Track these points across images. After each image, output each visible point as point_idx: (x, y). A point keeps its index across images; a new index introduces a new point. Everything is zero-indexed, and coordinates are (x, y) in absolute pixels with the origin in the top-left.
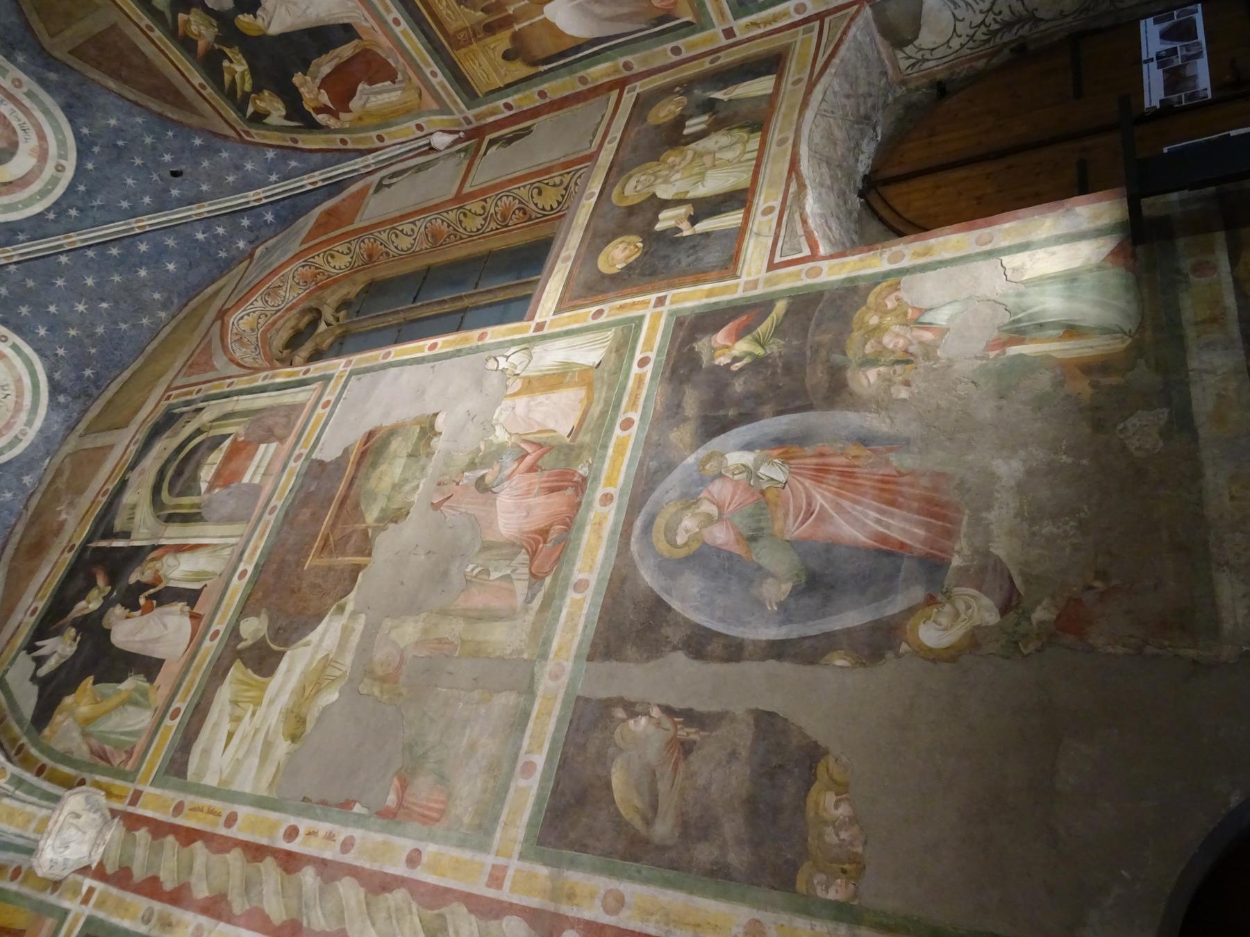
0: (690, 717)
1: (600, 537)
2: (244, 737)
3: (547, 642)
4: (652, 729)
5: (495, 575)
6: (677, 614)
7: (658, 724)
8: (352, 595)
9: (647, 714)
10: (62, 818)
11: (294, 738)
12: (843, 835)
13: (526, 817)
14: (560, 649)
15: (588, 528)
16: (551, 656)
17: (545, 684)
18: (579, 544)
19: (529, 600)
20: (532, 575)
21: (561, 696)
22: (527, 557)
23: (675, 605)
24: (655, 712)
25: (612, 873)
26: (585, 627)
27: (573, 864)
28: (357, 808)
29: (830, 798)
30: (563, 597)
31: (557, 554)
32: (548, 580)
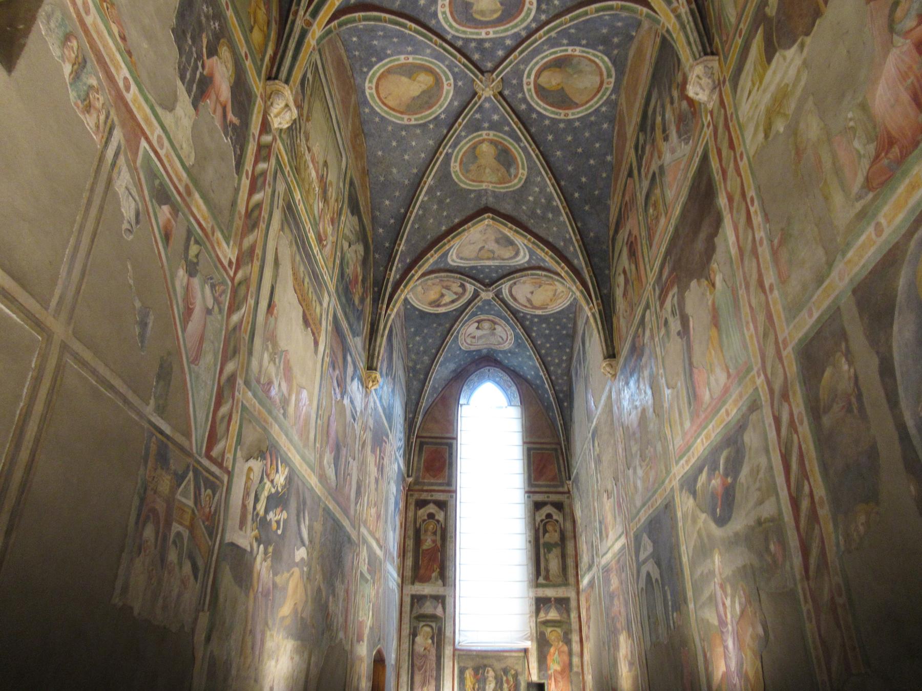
0: (859, 396)
1: (906, 202)
2: (753, 103)
3: (848, 245)
4: (846, 376)
5: (856, 144)
6: (891, 334)
7: (850, 378)
8: (808, 40)
9: (850, 366)
10: (694, 76)
11: (766, 136)
12: (855, 534)
13: (800, 335)
14: (849, 261)
15: (907, 181)
16: (845, 260)
17: (834, 274)
18: (896, 189)
19: (859, 198)
20: (867, 179)
21: (836, 292)
22: (874, 153)
23: (896, 328)
24: (852, 370)
25: (806, 408)
26: (864, 266)
27: (800, 382)
28: (768, 226)
29: (862, 519)
30: (868, 224)
31: (884, 178)
32: (871, 195)
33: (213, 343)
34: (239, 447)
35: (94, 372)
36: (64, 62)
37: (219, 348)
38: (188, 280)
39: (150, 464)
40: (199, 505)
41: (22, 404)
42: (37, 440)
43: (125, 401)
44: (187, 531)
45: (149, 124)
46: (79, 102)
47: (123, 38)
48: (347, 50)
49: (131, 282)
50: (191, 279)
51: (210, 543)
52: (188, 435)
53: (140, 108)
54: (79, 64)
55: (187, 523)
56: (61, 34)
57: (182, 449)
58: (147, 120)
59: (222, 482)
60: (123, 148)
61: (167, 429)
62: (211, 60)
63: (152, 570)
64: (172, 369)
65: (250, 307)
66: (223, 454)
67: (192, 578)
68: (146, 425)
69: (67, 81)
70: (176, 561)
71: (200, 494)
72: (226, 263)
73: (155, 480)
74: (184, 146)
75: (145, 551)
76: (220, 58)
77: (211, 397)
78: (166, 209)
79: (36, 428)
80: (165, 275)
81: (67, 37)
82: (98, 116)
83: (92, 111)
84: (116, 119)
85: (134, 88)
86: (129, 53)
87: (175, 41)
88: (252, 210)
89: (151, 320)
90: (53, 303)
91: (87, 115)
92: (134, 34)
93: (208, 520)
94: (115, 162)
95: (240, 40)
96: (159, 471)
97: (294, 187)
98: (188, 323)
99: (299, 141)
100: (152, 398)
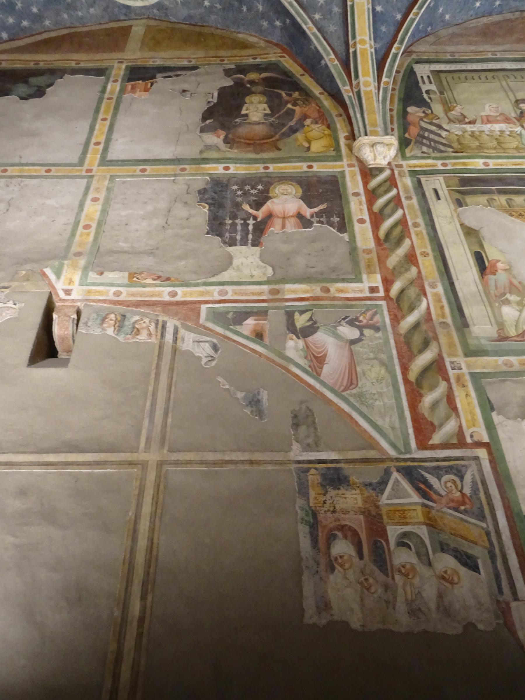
33: (376, 358)
34: (494, 414)
35: (201, 463)
36: (106, 330)
37: (391, 358)
38: (305, 342)
39: (312, 494)
40: (435, 497)
41: (130, 514)
42: (152, 530)
43: (251, 462)
44: (424, 528)
45: (207, 293)
46: (129, 336)
47: (159, 277)
48: (490, 14)
49: (227, 387)
50: (310, 339)
51: (484, 525)
52: (373, 445)
53: (191, 294)
54: (119, 321)
55: (421, 519)
56: (99, 321)
57: (366, 461)
58: (202, 294)
59: (477, 458)
60: (180, 326)
61: (334, 456)
62: (264, 208)
63: (366, 580)
64: (311, 410)
65: (437, 296)
66: (460, 433)
67: (463, 571)
68: (293, 467)
69: (114, 335)
70: (414, 560)
71: (430, 487)
72: (368, 294)
73: (328, 502)
74: (254, 273)
75: (342, 566)
76: (275, 197)
77: (398, 398)
78: (250, 322)
79: (148, 523)
80: (268, 359)
81: (104, 320)
82: (149, 330)
83: (141, 331)
84: (165, 319)
85: (180, 291)
86: (168, 279)
87: (213, 235)
88: (388, 235)
89: (264, 396)
90: (142, 445)
91: (138, 337)
92: (167, 269)
93: (463, 503)
94: (176, 338)
95: (294, 168)
96: (332, 492)
97: (464, 164)
98: (322, 368)
99: (444, 134)
100: (294, 442)
